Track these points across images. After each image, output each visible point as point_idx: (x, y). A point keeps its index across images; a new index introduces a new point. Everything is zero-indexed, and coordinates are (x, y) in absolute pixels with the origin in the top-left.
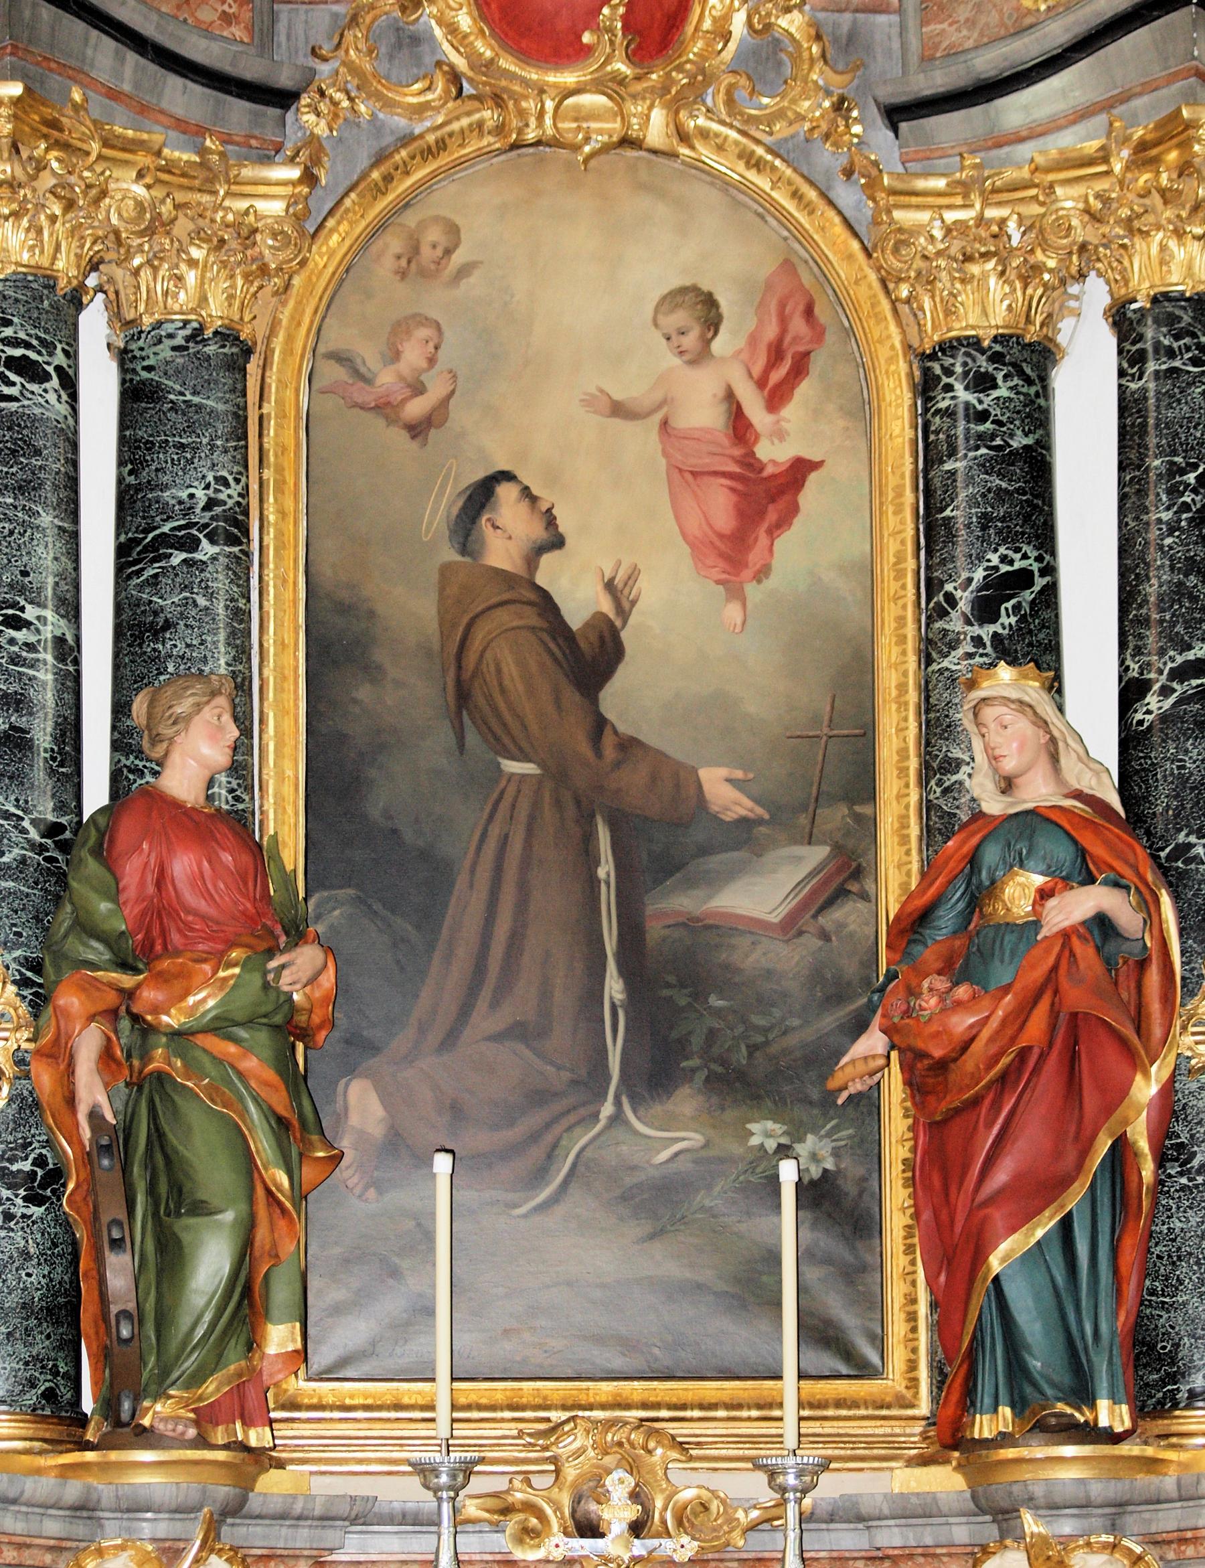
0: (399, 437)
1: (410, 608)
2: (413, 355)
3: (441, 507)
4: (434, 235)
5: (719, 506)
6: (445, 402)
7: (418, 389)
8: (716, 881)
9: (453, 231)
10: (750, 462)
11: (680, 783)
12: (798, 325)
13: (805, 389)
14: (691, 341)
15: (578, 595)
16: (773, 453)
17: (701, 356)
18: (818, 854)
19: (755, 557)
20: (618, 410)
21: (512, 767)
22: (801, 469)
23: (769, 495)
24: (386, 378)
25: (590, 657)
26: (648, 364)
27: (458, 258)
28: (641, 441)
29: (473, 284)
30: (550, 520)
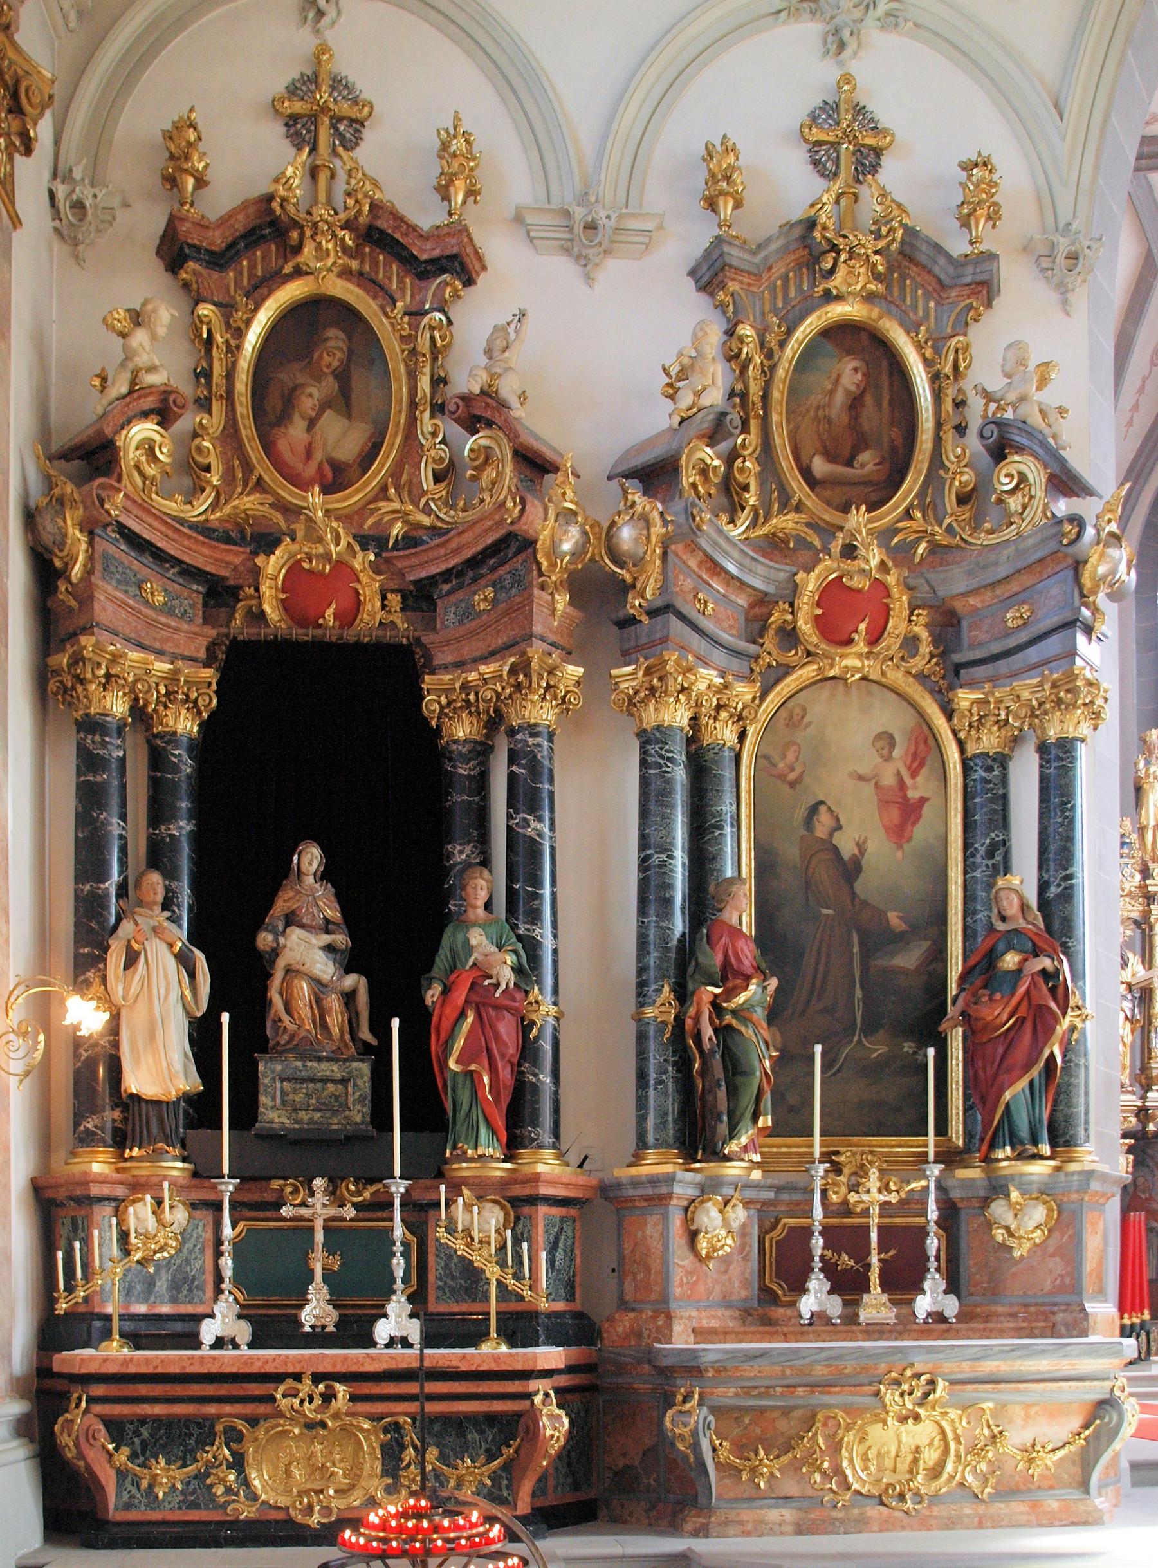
0: (786, 789)
1: (790, 851)
2: (791, 756)
3: (800, 813)
4: (797, 710)
5: (895, 814)
6: (801, 775)
7: (792, 769)
8: (893, 954)
9: (804, 709)
10: (905, 797)
11: (881, 915)
12: (922, 746)
13: (924, 771)
14: (885, 752)
15: (846, 846)
16: (913, 794)
17: (888, 758)
18: (926, 945)
19: (906, 834)
20: (861, 778)
21: (825, 911)
22: (923, 800)
23: (911, 811)
24: (781, 765)
25: (851, 870)
26: (869, 761)
27: (807, 719)
28: (868, 790)
29: (811, 730)
30: (838, 820)
